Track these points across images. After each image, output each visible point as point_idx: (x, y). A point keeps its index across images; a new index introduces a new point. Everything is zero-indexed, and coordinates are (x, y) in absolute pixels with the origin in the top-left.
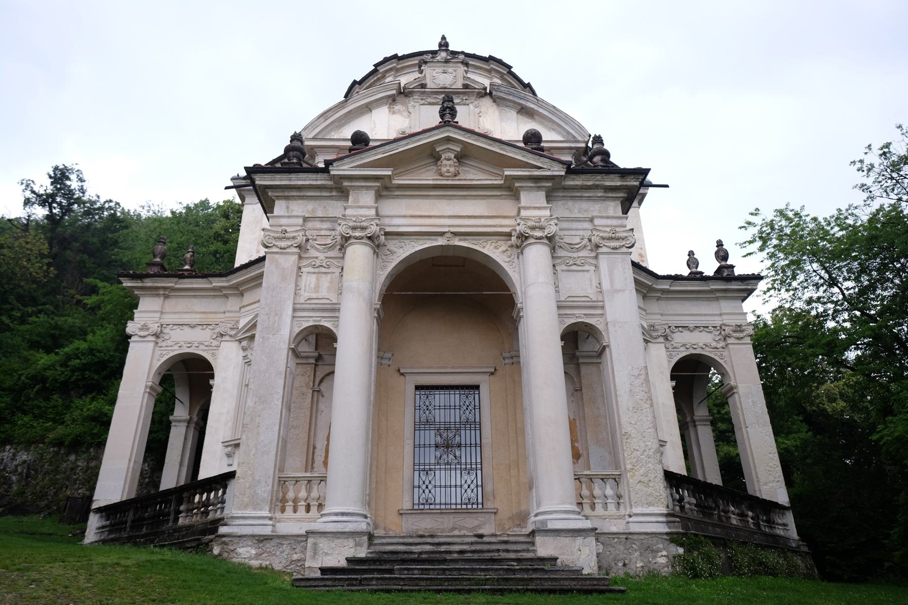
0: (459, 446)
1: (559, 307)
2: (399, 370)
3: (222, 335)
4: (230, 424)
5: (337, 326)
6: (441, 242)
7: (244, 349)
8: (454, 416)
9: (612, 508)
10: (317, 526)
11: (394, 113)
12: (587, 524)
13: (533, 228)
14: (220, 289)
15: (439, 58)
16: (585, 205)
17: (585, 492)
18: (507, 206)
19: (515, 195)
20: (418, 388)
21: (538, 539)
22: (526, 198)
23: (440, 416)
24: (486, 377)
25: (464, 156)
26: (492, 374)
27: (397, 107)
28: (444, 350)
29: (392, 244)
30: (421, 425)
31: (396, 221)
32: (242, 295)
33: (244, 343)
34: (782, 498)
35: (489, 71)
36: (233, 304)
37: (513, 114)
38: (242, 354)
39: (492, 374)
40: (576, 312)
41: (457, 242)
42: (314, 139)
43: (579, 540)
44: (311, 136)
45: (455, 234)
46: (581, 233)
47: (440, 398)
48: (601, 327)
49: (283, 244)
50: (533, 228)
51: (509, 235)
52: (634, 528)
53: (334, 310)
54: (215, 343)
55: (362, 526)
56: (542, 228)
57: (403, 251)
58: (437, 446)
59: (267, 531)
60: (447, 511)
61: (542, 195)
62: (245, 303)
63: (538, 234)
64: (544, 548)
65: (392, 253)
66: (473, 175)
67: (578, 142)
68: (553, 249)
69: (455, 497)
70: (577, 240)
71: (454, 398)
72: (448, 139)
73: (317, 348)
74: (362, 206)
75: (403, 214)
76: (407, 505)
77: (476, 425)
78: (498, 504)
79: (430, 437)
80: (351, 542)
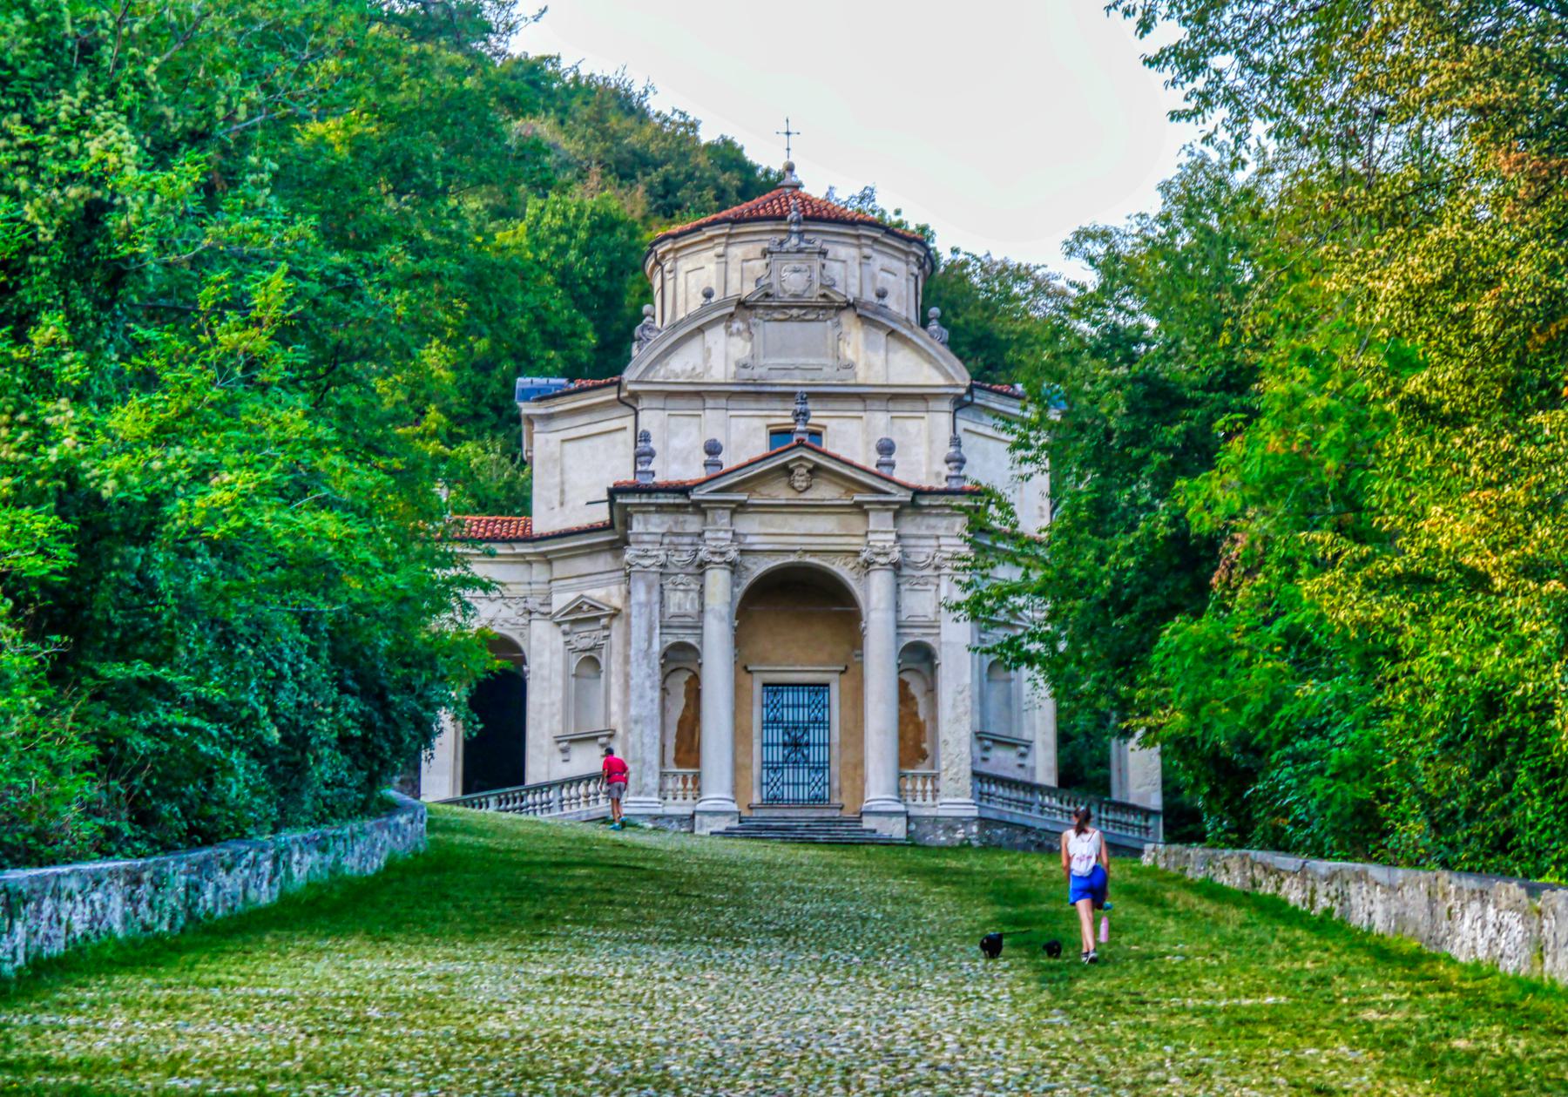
0: (808, 744)
1: (898, 627)
2: (745, 668)
3: (530, 613)
4: (558, 717)
5: (701, 643)
6: (792, 559)
7: (565, 633)
8: (803, 715)
9: (929, 799)
10: (700, 807)
11: (731, 334)
12: (901, 808)
13: (878, 554)
14: (522, 555)
15: (787, 246)
16: (932, 521)
17: (909, 786)
18: (856, 522)
19: (866, 513)
20: (765, 685)
21: (865, 818)
22: (873, 518)
23: (789, 715)
24: (836, 676)
25: (815, 470)
26: (842, 672)
27: (737, 325)
28: (796, 656)
29: (749, 561)
30: (770, 723)
31: (749, 539)
32: (550, 562)
33: (566, 627)
34: (1155, 802)
35: (858, 237)
36: (539, 573)
37: (882, 335)
38: (562, 639)
39: (842, 672)
40: (915, 631)
41: (809, 559)
42: (637, 382)
43: (894, 819)
44: (634, 378)
45: (806, 552)
46: (927, 550)
47: (788, 697)
48: (935, 645)
49: (647, 562)
50: (878, 554)
51: (857, 553)
52: (941, 813)
53: (698, 627)
54: (522, 621)
55: (735, 807)
56: (886, 554)
57: (758, 567)
58: (785, 745)
59: (659, 811)
60: (796, 803)
61: (890, 515)
62: (556, 574)
63: (882, 560)
64: (869, 823)
65: (747, 569)
66: (825, 492)
67: (957, 386)
68: (897, 575)
69: (803, 793)
70: (922, 558)
71: (804, 697)
72: (801, 458)
73: (680, 661)
74: (719, 533)
75: (755, 529)
76: (756, 799)
77: (823, 724)
78: (844, 801)
79: (778, 736)
80: (728, 818)
